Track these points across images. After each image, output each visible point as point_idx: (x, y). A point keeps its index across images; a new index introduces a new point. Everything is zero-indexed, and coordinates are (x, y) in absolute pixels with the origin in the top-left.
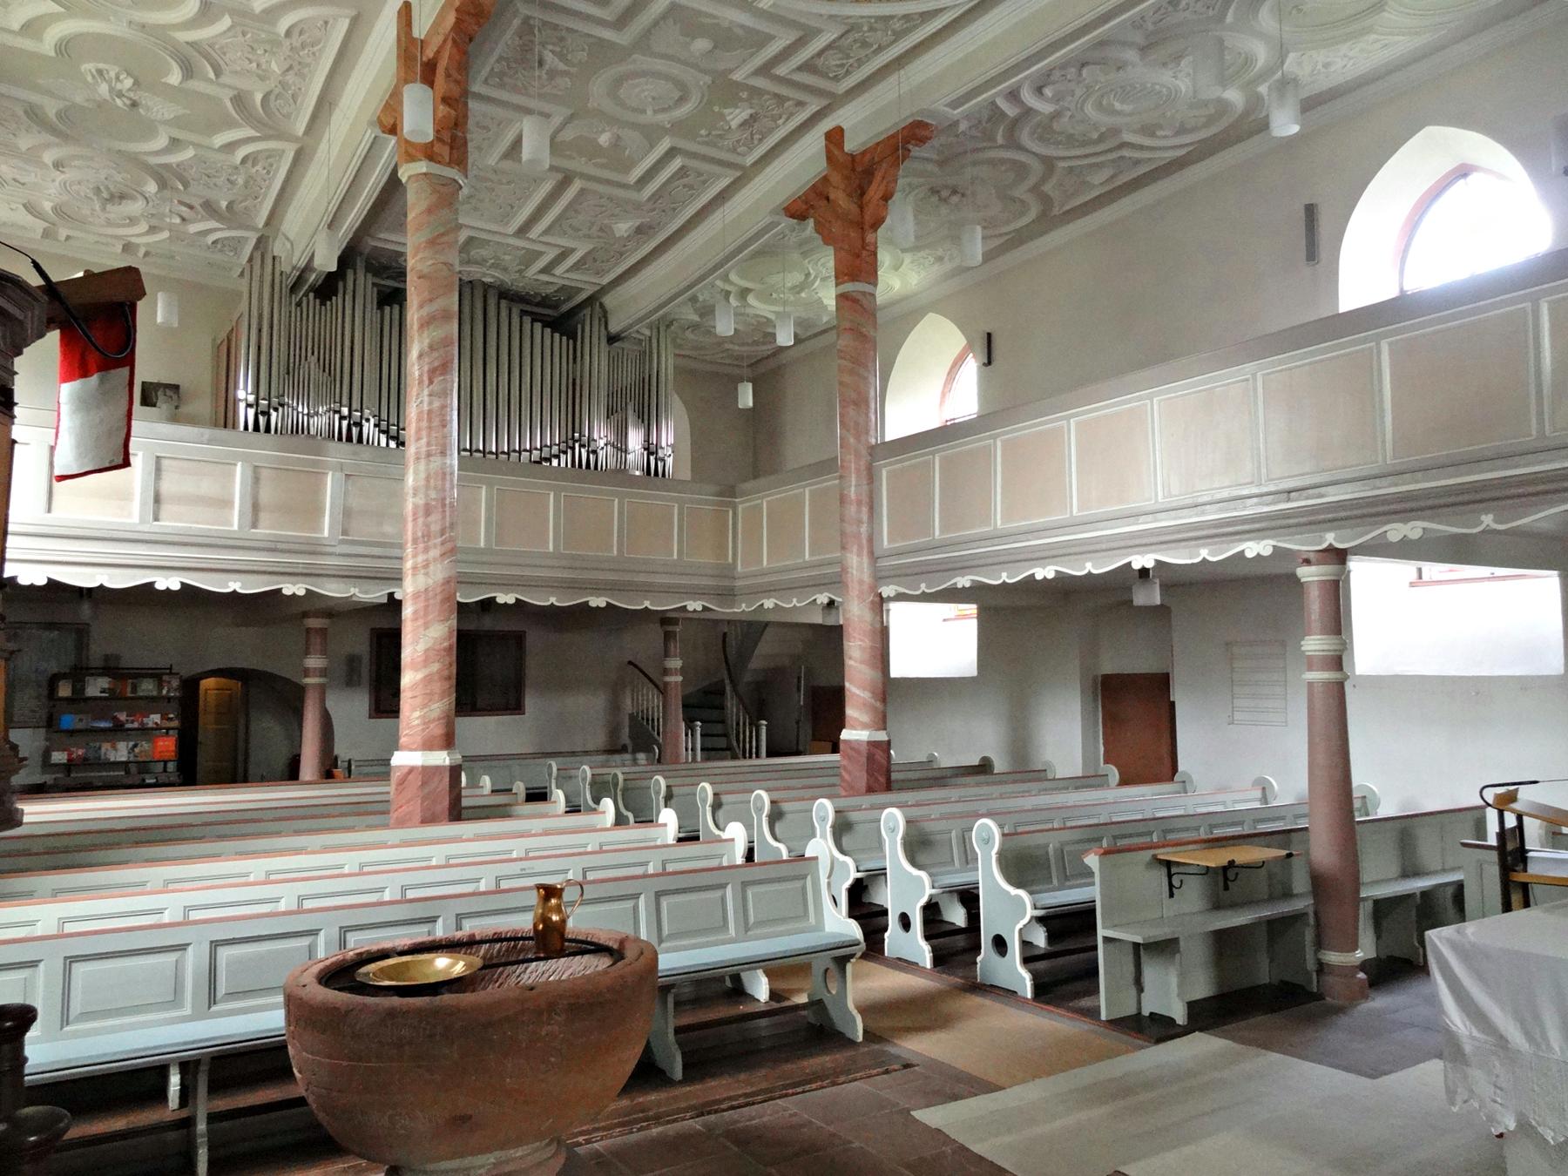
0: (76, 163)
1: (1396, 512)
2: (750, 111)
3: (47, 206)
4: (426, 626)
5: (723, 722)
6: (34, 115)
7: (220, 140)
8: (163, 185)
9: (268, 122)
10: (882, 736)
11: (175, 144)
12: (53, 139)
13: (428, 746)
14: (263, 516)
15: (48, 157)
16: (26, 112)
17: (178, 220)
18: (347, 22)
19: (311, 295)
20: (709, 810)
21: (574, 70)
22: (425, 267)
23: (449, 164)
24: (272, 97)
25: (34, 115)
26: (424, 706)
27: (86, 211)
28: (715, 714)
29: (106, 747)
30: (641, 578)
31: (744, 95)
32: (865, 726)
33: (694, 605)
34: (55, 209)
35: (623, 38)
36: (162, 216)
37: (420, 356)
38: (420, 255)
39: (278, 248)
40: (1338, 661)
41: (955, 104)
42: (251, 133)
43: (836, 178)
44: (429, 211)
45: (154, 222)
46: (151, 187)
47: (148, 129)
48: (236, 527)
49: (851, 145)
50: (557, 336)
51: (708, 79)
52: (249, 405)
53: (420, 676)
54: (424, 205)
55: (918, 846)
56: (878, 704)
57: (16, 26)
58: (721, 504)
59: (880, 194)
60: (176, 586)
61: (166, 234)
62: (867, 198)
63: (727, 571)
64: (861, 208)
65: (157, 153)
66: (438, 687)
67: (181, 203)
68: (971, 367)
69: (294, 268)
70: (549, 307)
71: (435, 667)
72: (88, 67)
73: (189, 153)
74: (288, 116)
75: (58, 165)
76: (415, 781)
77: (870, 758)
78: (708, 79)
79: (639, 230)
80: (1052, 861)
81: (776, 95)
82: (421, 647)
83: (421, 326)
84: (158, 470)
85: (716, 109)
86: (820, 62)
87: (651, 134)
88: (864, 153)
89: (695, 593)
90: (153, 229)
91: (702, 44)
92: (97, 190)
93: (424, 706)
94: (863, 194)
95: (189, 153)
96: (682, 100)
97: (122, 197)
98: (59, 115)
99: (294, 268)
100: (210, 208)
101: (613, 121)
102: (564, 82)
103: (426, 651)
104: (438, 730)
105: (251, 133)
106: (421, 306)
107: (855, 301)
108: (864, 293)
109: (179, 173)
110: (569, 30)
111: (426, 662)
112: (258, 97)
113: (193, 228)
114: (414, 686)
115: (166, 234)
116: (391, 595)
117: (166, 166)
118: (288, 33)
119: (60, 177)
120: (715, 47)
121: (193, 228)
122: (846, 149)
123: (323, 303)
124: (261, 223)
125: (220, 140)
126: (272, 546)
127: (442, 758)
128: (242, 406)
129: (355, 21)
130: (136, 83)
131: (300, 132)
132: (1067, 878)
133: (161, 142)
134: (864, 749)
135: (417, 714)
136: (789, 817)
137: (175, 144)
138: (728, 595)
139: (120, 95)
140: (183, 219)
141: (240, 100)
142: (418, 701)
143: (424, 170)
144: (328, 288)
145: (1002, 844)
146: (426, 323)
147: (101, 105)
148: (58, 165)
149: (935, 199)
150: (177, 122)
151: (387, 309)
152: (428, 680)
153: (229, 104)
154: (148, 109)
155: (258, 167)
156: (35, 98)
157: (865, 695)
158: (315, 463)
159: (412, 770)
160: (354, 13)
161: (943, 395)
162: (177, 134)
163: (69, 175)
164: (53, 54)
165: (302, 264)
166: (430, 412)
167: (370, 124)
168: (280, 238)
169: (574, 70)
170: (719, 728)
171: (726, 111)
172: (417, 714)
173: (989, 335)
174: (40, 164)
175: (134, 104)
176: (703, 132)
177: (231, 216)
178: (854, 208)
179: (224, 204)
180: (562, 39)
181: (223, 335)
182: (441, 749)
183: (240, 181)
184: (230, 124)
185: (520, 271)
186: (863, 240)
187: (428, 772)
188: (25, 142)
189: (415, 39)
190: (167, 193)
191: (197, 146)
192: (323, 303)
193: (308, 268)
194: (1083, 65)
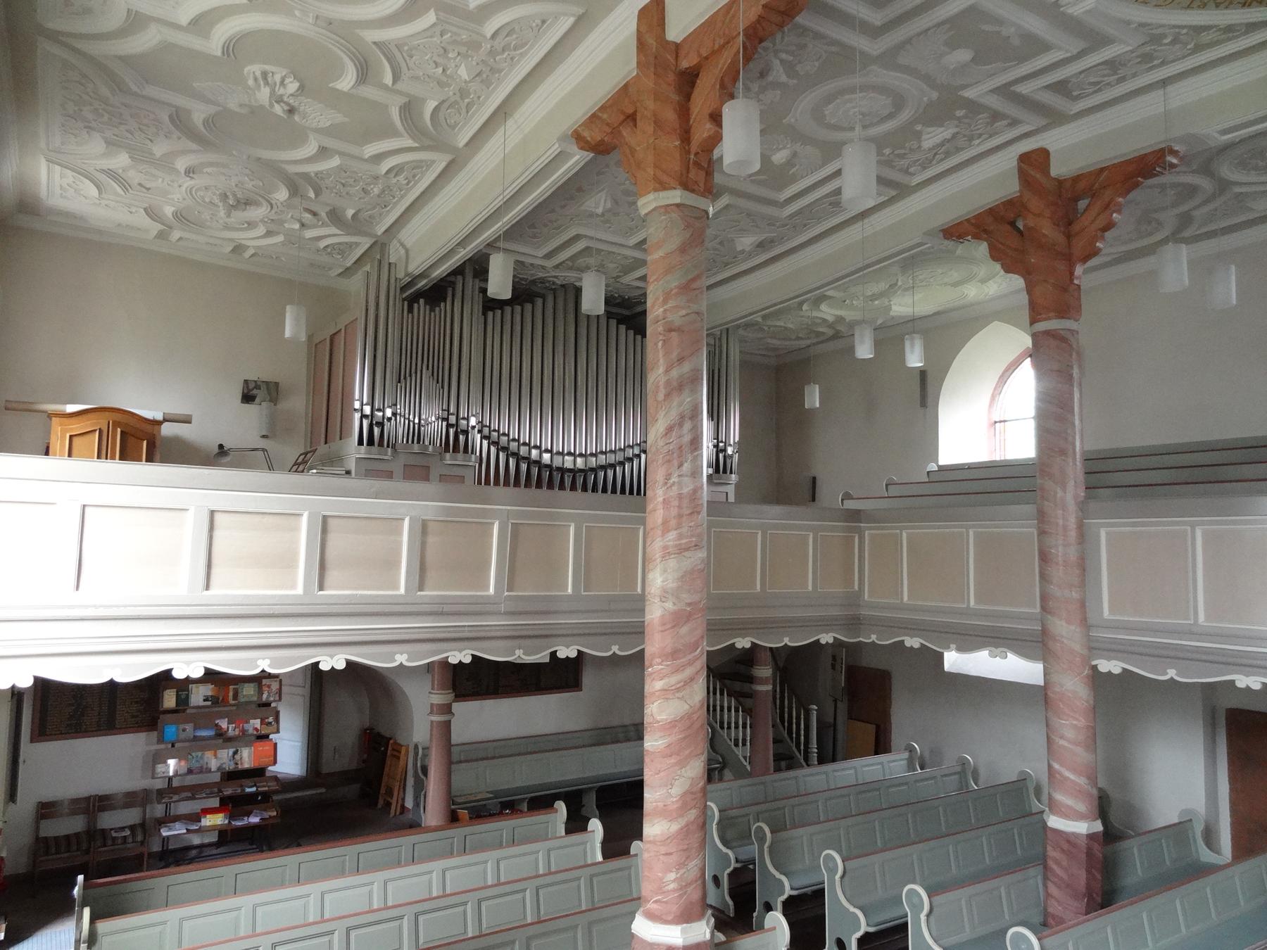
0: (209, 170)
3: (169, 211)
4: (682, 764)
6: (180, 121)
7: (371, 150)
8: (294, 190)
9: (429, 134)
11: (323, 152)
12: (194, 146)
14: (431, 576)
15: (181, 164)
16: (170, 117)
17: (297, 226)
18: (572, 20)
19: (422, 301)
22: (676, 318)
24: (446, 105)
25: (180, 121)
26: (681, 865)
27: (206, 216)
29: (209, 755)
30: (780, 614)
31: (960, 113)
32: (1080, 817)
33: (826, 638)
34: (175, 215)
35: (873, 47)
36: (281, 222)
38: (671, 304)
42: (409, 143)
44: (683, 250)
45: (273, 227)
46: (282, 194)
47: (298, 137)
48: (402, 591)
49: (1059, 169)
50: (631, 333)
52: (363, 416)
53: (675, 827)
54: (674, 243)
57: (184, 20)
60: (341, 665)
61: (280, 238)
62: (1076, 227)
63: (853, 599)
64: (1069, 236)
65: (296, 162)
67: (307, 210)
69: (407, 275)
70: (628, 308)
72: (256, 68)
73: (335, 162)
74: (453, 127)
75: (190, 172)
78: (935, 95)
79: (761, 246)
82: (677, 791)
84: (324, 531)
89: (826, 624)
90: (269, 234)
92: (224, 197)
93: (681, 865)
94: (1070, 223)
95: (335, 162)
97: (247, 203)
98: (206, 122)
99: (407, 275)
100: (335, 217)
103: (685, 794)
105: (409, 143)
107: (1063, 339)
108: (1072, 332)
109: (316, 183)
112: (431, 105)
113: (309, 234)
114: (666, 840)
115: (280, 238)
116: (553, 654)
117: (305, 176)
118: (494, 36)
119: (188, 183)
121: (309, 234)
122: (1054, 172)
123: (432, 310)
124: (380, 230)
125: (371, 150)
126: (435, 608)
128: (357, 416)
129: (580, 19)
130: (302, 88)
131: (461, 144)
133: (310, 149)
134: (1083, 843)
135: (672, 876)
137: (323, 152)
138: (854, 623)
139: (280, 100)
140: (303, 225)
141: (409, 109)
142: (674, 858)
143: (678, 201)
144: (436, 293)
147: (256, 111)
148: (190, 172)
150: (329, 132)
151: (490, 314)
153: (395, 113)
154: (304, 116)
155: (401, 178)
156: (182, 101)
157: (1082, 781)
158: (484, 514)
160: (581, 11)
162: (330, 143)
163: (198, 181)
164: (219, 53)
165: (417, 272)
166: (680, 497)
168: (395, 241)
172: (672, 876)
174: (174, 170)
175: (291, 111)
177: (356, 225)
178: (1061, 239)
179: (350, 213)
181: (326, 335)
183: (376, 191)
184: (391, 133)
185: (618, 277)
188: (159, 149)
189: (668, 42)
190: (297, 200)
191: (341, 154)
192: (432, 310)
193: (422, 276)
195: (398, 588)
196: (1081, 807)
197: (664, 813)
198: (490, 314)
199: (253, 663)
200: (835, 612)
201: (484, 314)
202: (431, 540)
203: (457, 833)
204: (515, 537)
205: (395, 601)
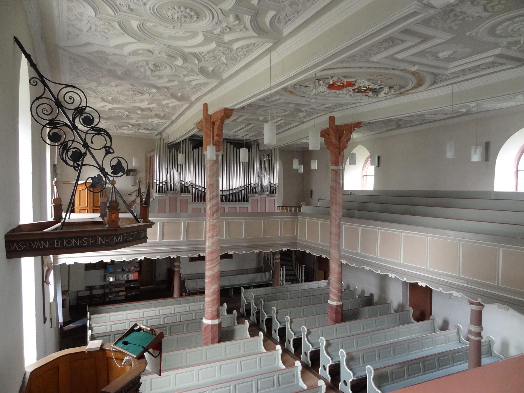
1: (501, 301)
4: (212, 285)
5: (291, 261)
10: (340, 303)
13: (213, 318)
20: (289, 324)
26: (212, 307)
28: (289, 263)
29: (121, 276)
37: (210, 208)
39: (164, 133)
40: (479, 335)
43: (331, 132)
49: (337, 123)
52: (157, 184)
53: (210, 299)
55: (350, 360)
56: (339, 294)
58: (294, 218)
59: (345, 140)
64: (339, 142)
66: (216, 302)
68: (371, 169)
71: (215, 296)
76: (209, 329)
77: (337, 310)
80: (389, 376)
82: (211, 291)
83: (210, 199)
88: (341, 126)
94: (340, 138)
101: (263, 115)
104: (215, 314)
106: (210, 194)
111: (213, 294)
114: (208, 302)
116: (199, 255)
122: (336, 124)
127: (216, 322)
132: (393, 380)
136: (312, 333)
138: (295, 244)
142: (210, 306)
145: (375, 372)
146: (212, 199)
151: (195, 150)
152: (213, 300)
157: (336, 292)
158: (179, 220)
159: (208, 325)
161: (363, 167)
167: (194, 124)
170: (291, 268)
173: (379, 157)
178: (337, 143)
182: (216, 319)
187: (213, 326)
195: (157, 239)
196: (335, 298)
197: (209, 297)
198: (195, 150)
199: (122, 258)
200: (289, 242)
201: (193, 150)
202: (165, 227)
203: (182, 299)
204: (188, 225)
205: (156, 243)
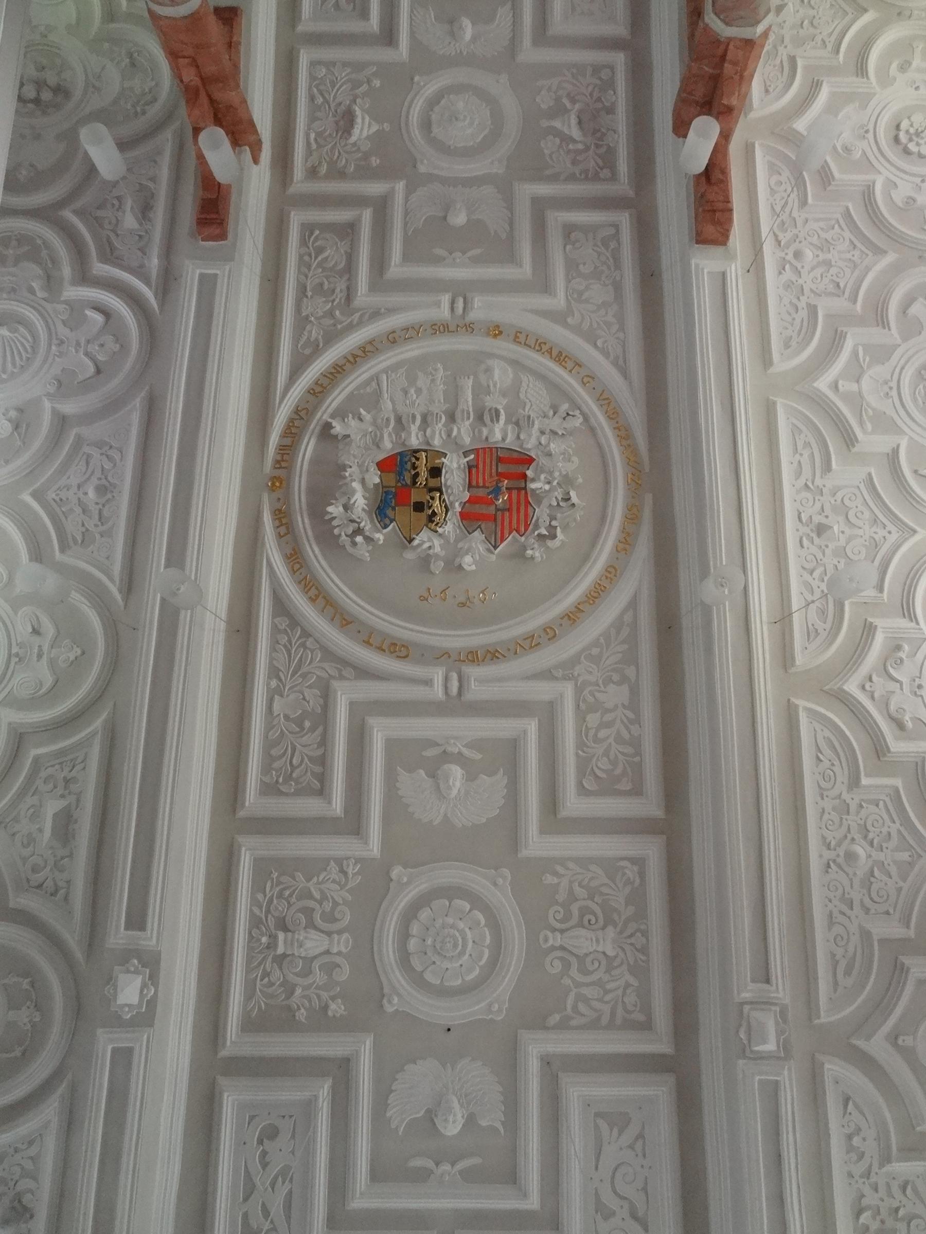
2: (353, 139)
21: (545, 123)
23: (730, 40)
41: (208, 285)
51: (422, 169)
78: (422, 169)
81: (342, 175)
85: (386, 127)
86: (343, 247)
87: (426, 60)
91: (459, 219)
96: (427, 125)
102: (545, 101)
110: (572, 178)
120: (445, 218)
149: (52, 80)
169: (545, 123)
171: (375, 128)
176: (377, 83)
180: (574, 162)
186: (197, 67)
194: (98, 371)
